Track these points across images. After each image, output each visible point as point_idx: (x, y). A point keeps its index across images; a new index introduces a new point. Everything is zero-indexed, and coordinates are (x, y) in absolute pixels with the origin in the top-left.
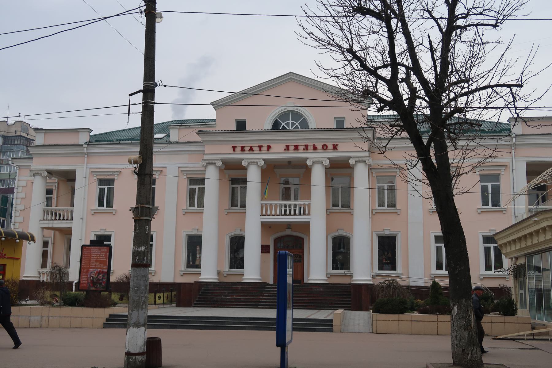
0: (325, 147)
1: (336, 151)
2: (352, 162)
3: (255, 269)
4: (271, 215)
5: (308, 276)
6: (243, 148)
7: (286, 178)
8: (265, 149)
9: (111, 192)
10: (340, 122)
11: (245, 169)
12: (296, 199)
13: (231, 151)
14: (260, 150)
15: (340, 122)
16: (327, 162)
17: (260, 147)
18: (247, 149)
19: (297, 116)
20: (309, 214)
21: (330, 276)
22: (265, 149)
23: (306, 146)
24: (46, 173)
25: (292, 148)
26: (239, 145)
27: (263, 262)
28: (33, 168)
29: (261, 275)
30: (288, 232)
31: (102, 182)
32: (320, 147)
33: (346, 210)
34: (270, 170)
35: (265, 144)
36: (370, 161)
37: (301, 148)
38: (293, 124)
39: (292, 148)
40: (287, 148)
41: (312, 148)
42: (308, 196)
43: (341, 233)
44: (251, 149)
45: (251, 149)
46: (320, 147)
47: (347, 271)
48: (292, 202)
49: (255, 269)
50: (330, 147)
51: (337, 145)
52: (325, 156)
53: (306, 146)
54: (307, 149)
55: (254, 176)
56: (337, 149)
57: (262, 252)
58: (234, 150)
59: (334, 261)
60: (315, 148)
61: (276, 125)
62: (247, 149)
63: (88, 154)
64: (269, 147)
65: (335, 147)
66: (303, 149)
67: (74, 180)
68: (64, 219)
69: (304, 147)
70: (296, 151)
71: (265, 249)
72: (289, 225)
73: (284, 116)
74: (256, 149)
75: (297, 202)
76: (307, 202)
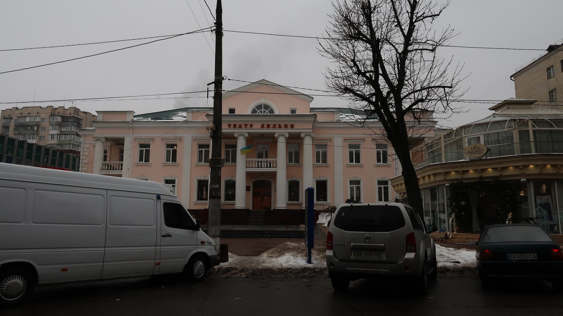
0: (286, 126)
2: (302, 135)
3: (241, 201)
4: (252, 167)
5: (275, 204)
6: (235, 126)
7: (262, 144)
8: (249, 126)
9: (148, 152)
10: (293, 111)
11: (236, 139)
12: (266, 157)
13: (227, 127)
15: (293, 111)
16: (287, 135)
17: (246, 125)
18: (238, 126)
19: (267, 107)
20: (276, 167)
21: (288, 204)
22: (249, 126)
23: (275, 125)
24: (104, 140)
25: (265, 126)
26: (232, 124)
27: (247, 196)
28: (95, 136)
29: (246, 205)
30: (262, 178)
31: (142, 146)
32: (283, 126)
33: (297, 164)
34: (252, 140)
35: (249, 124)
36: (313, 135)
37: (271, 126)
38: (264, 112)
39: (265, 126)
41: (278, 126)
42: (275, 156)
43: (294, 179)
44: (240, 126)
45: (240, 126)
46: (283, 126)
47: (298, 202)
48: (264, 159)
49: (241, 201)
50: (289, 126)
52: (286, 132)
53: (275, 125)
55: (241, 144)
57: (247, 190)
59: (290, 196)
60: (280, 127)
61: (254, 111)
62: (238, 126)
63: (132, 128)
64: (251, 126)
65: (292, 126)
67: (123, 144)
68: (116, 169)
71: (248, 189)
72: (262, 174)
73: (259, 107)
74: (243, 126)
75: (268, 160)
76: (274, 160)
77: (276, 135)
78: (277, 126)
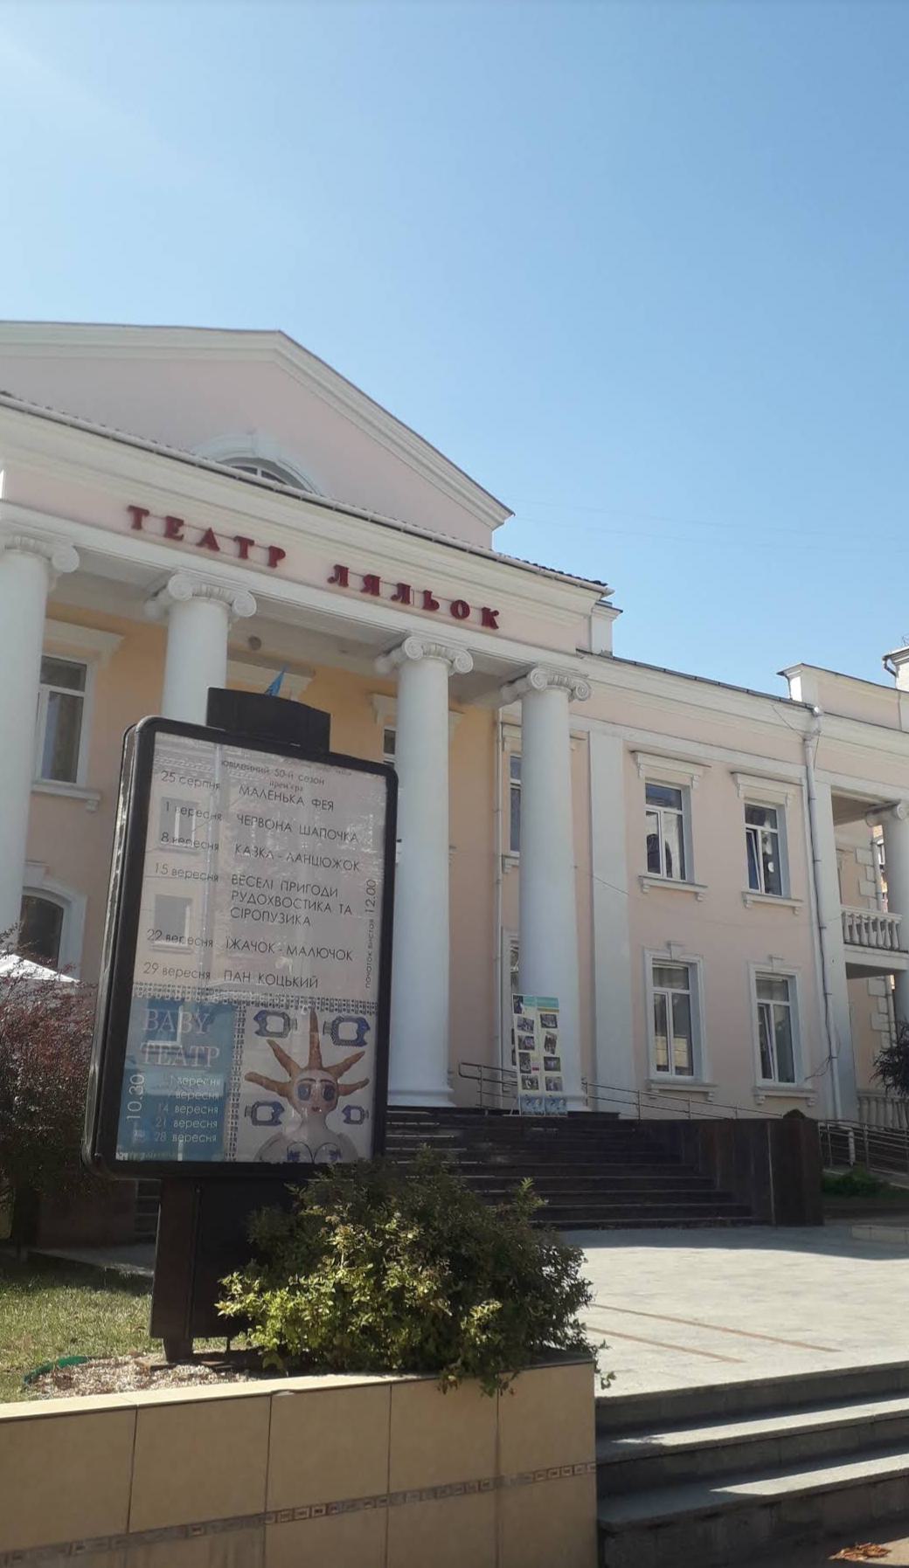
1: (489, 630)
8: (258, 555)
13: (126, 520)
14: (243, 554)
16: (466, 665)
22: (258, 555)
35: (266, 538)
39: (355, 582)
40: (340, 575)
51: (496, 613)
52: (468, 643)
54: (406, 600)
56: (493, 625)
58: (137, 525)
60: (430, 604)
64: (276, 555)
65: (489, 619)
66: (394, 598)
69: (394, 591)
70: (368, 596)
77: (411, 647)
78: (417, 599)
